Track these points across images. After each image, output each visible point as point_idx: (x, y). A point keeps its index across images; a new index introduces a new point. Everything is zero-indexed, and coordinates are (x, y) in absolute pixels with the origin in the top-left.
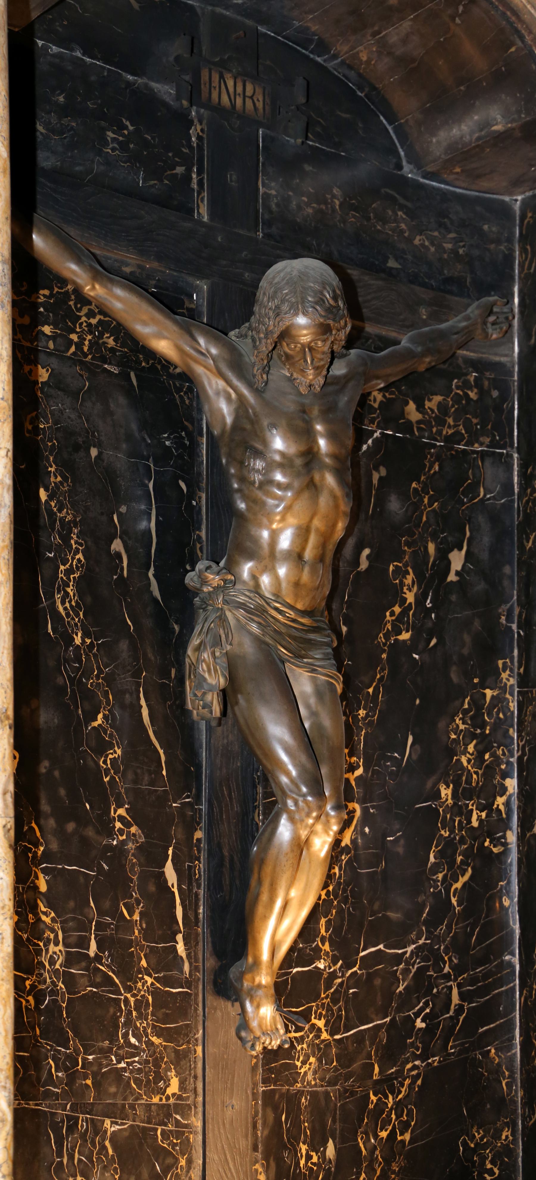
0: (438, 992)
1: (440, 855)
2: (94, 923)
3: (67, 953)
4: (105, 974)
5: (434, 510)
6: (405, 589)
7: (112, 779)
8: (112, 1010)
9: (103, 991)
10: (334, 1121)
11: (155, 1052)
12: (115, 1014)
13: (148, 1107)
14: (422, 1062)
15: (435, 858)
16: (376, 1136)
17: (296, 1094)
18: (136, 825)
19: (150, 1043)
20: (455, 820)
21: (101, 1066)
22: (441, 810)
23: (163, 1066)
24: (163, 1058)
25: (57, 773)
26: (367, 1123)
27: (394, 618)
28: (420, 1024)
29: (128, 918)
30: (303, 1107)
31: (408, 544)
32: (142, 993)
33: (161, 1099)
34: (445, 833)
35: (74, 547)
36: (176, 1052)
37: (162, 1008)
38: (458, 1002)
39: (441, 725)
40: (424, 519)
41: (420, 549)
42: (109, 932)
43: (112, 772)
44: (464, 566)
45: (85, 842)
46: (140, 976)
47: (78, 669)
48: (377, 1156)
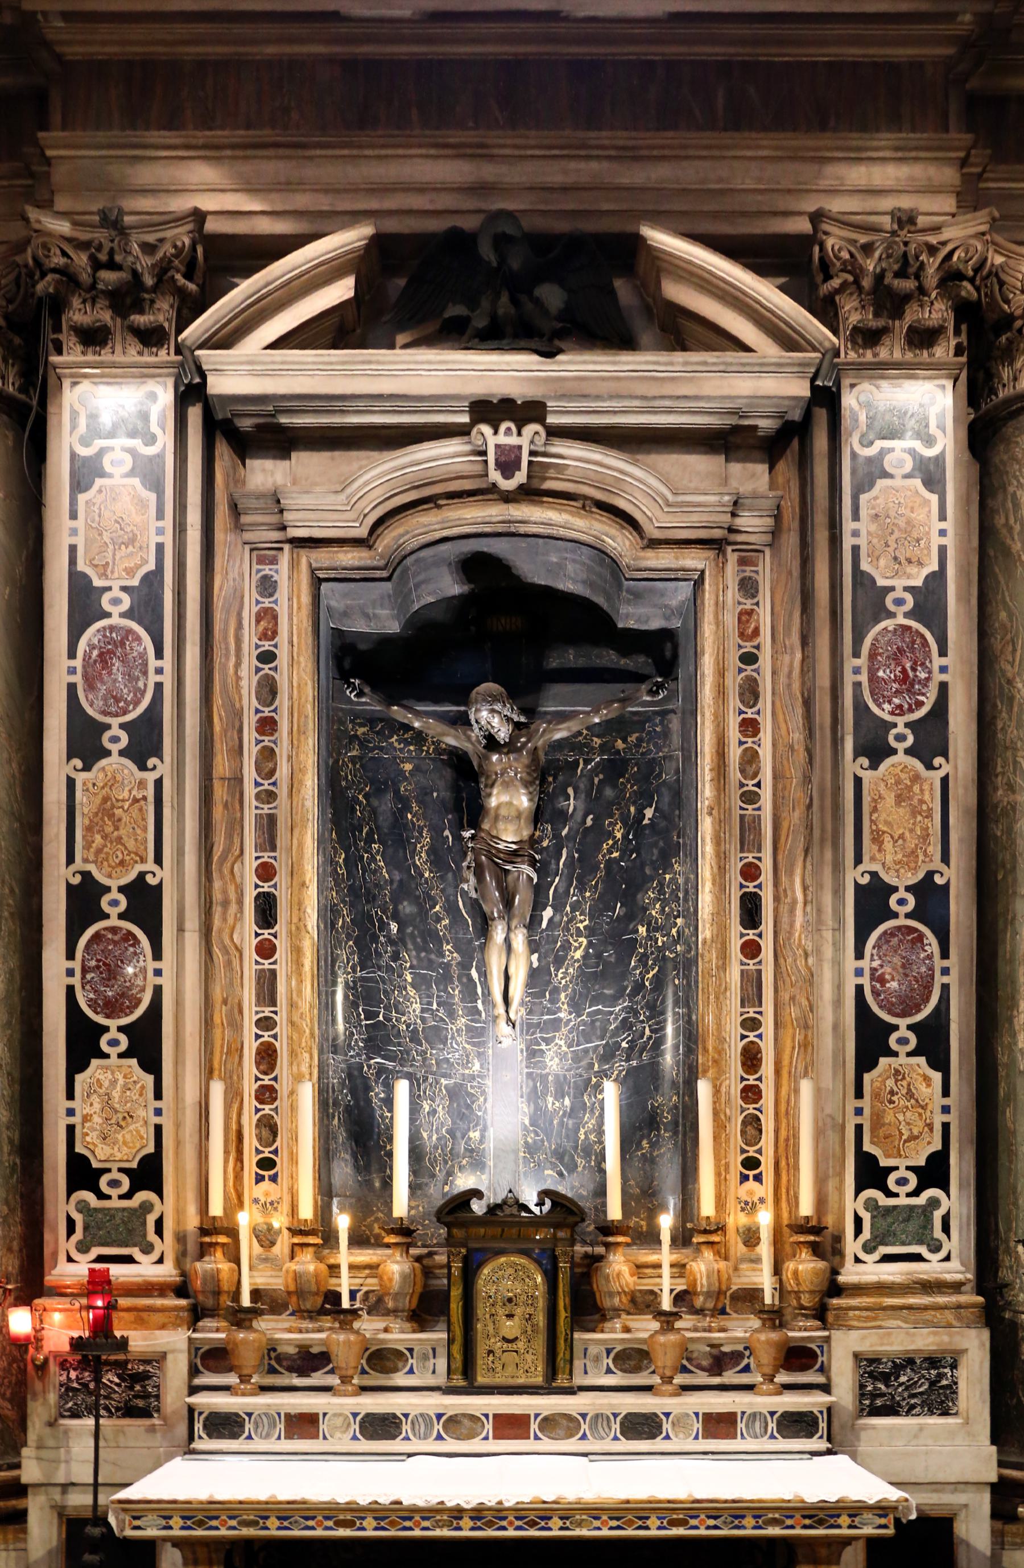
28: (624, 1045)
39: (639, 896)
45: (430, 961)
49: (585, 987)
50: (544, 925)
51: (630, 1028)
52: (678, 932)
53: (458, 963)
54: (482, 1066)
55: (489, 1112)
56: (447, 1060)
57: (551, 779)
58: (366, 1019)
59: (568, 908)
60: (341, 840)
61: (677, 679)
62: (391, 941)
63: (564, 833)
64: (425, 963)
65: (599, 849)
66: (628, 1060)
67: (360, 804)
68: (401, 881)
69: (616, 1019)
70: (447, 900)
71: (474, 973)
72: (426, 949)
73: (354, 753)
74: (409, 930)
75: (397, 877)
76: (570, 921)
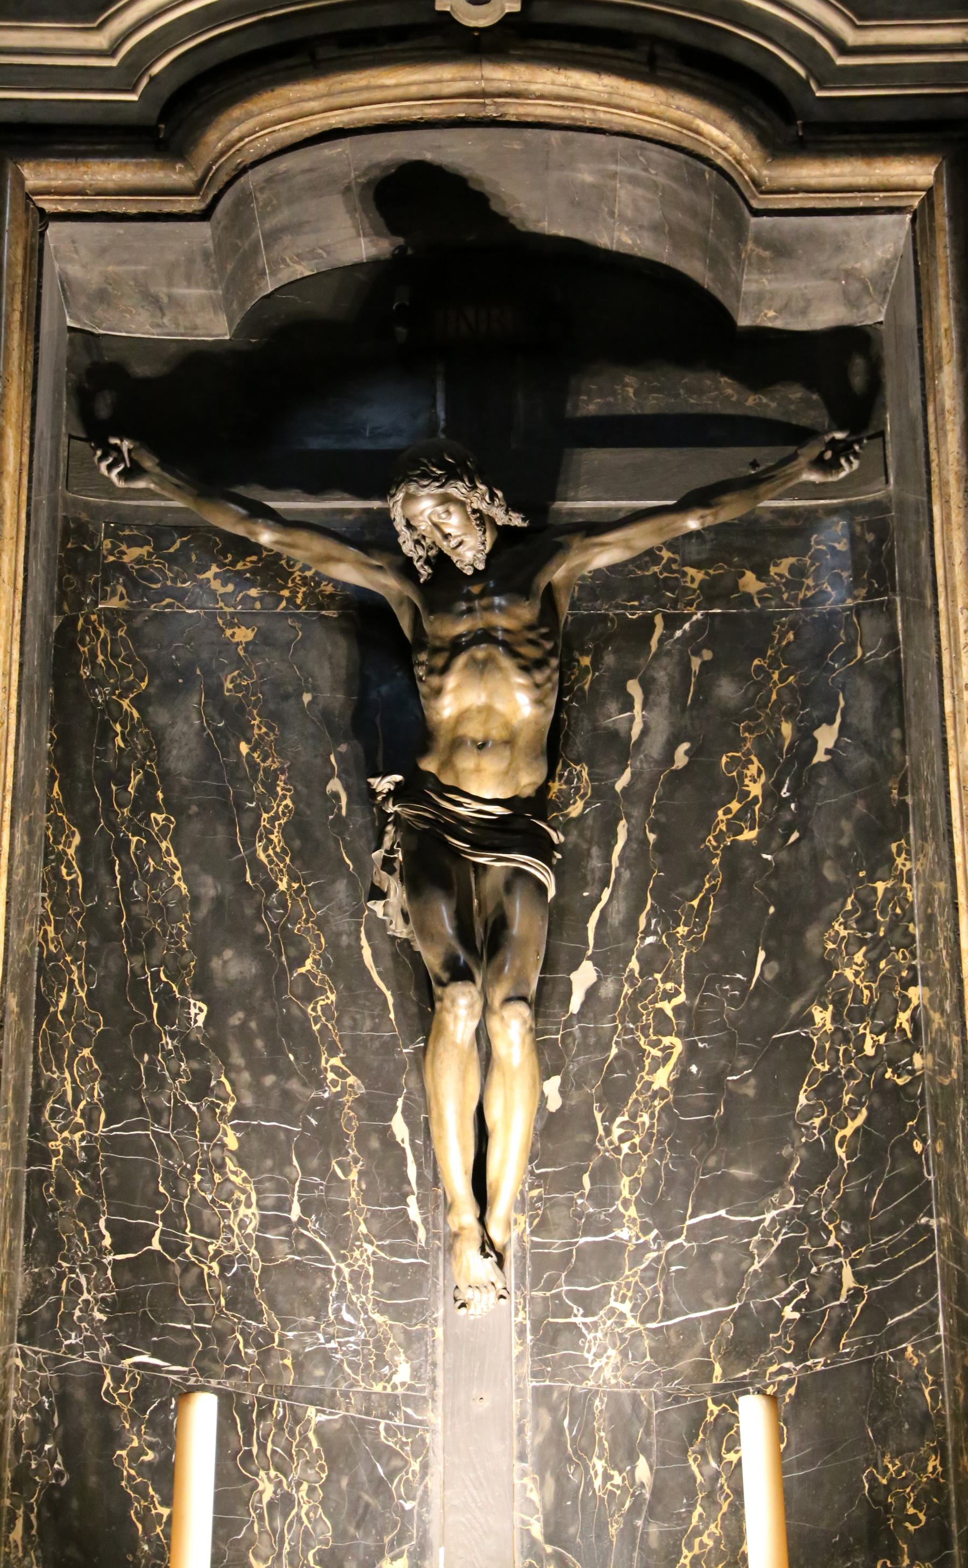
0: (819, 1271)
1: (818, 1093)
2: (297, 1184)
3: (263, 1216)
4: (311, 1242)
5: (789, 686)
6: (747, 781)
7: (324, 1026)
8: (319, 1282)
9: (309, 1260)
10: (647, 1432)
11: (377, 1332)
12: (323, 1286)
13: (367, 1396)
14: (796, 1364)
15: (807, 1098)
16: (719, 1459)
17: (586, 1394)
18: (355, 1074)
19: (370, 1322)
20: (838, 1051)
21: (304, 1345)
22: (815, 1039)
23: (388, 1348)
24: (387, 1340)
25: (253, 1025)
26: (703, 1440)
27: (730, 816)
28: (789, 1313)
29: (342, 1177)
30: (597, 1412)
31: (749, 729)
32: (360, 1263)
33: (385, 1388)
34: (824, 1067)
35: (280, 793)
36: (406, 1332)
37: (387, 1280)
38: (853, 1285)
39: (811, 934)
40: (774, 697)
41: (768, 732)
42: (317, 1194)
43: (323, 1019)
44: (837, 743)
45: (287, 1095)
46: (358, 1243)
47: (283, 915)
48: (722, 1486)
49: (680, 1160)
50: (575, 1005)
51: (803, 1270)
52: (913, 1020)
53: (359, 1101)
54: (416, 1373)
55: (436, 1500)
56: (326, 1357)
57: (586, 661)
58: (117, 1248)
59: (634, 965)
60: (69, 804)
61: (882, 434)
62: (189, 1048)
63: (620, 785)
64: (274, 1104)
65: (708, 822)
66: (800, 1355)
67: (124, 718)
68: (219, 902)
69: (765, 1244)
70: (333, 945)
71: (399, 1128)
72: (273, 1067)
73: (114, 603)
74: (236, 1019)
75: (210, 888)
76: (639, 995)
